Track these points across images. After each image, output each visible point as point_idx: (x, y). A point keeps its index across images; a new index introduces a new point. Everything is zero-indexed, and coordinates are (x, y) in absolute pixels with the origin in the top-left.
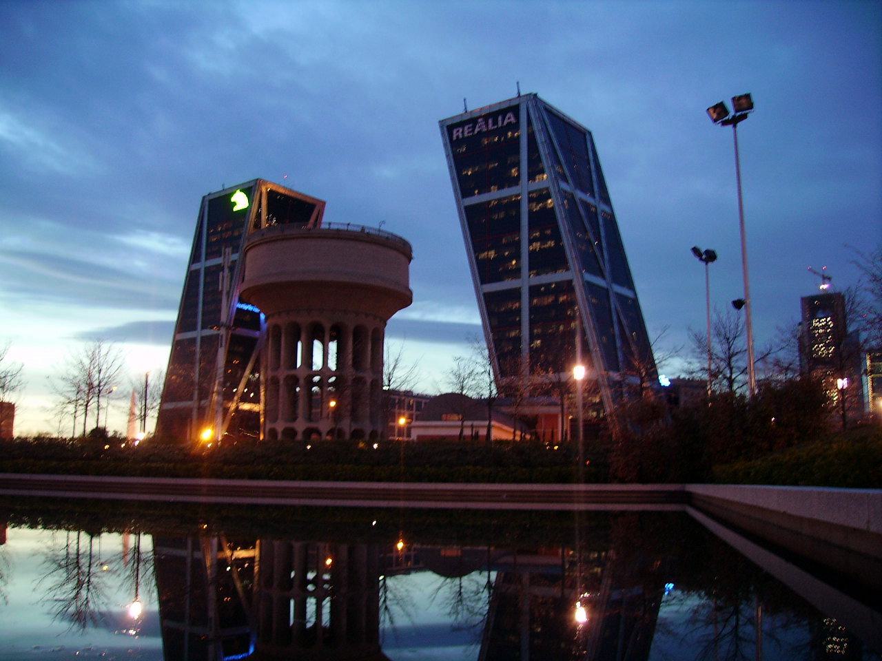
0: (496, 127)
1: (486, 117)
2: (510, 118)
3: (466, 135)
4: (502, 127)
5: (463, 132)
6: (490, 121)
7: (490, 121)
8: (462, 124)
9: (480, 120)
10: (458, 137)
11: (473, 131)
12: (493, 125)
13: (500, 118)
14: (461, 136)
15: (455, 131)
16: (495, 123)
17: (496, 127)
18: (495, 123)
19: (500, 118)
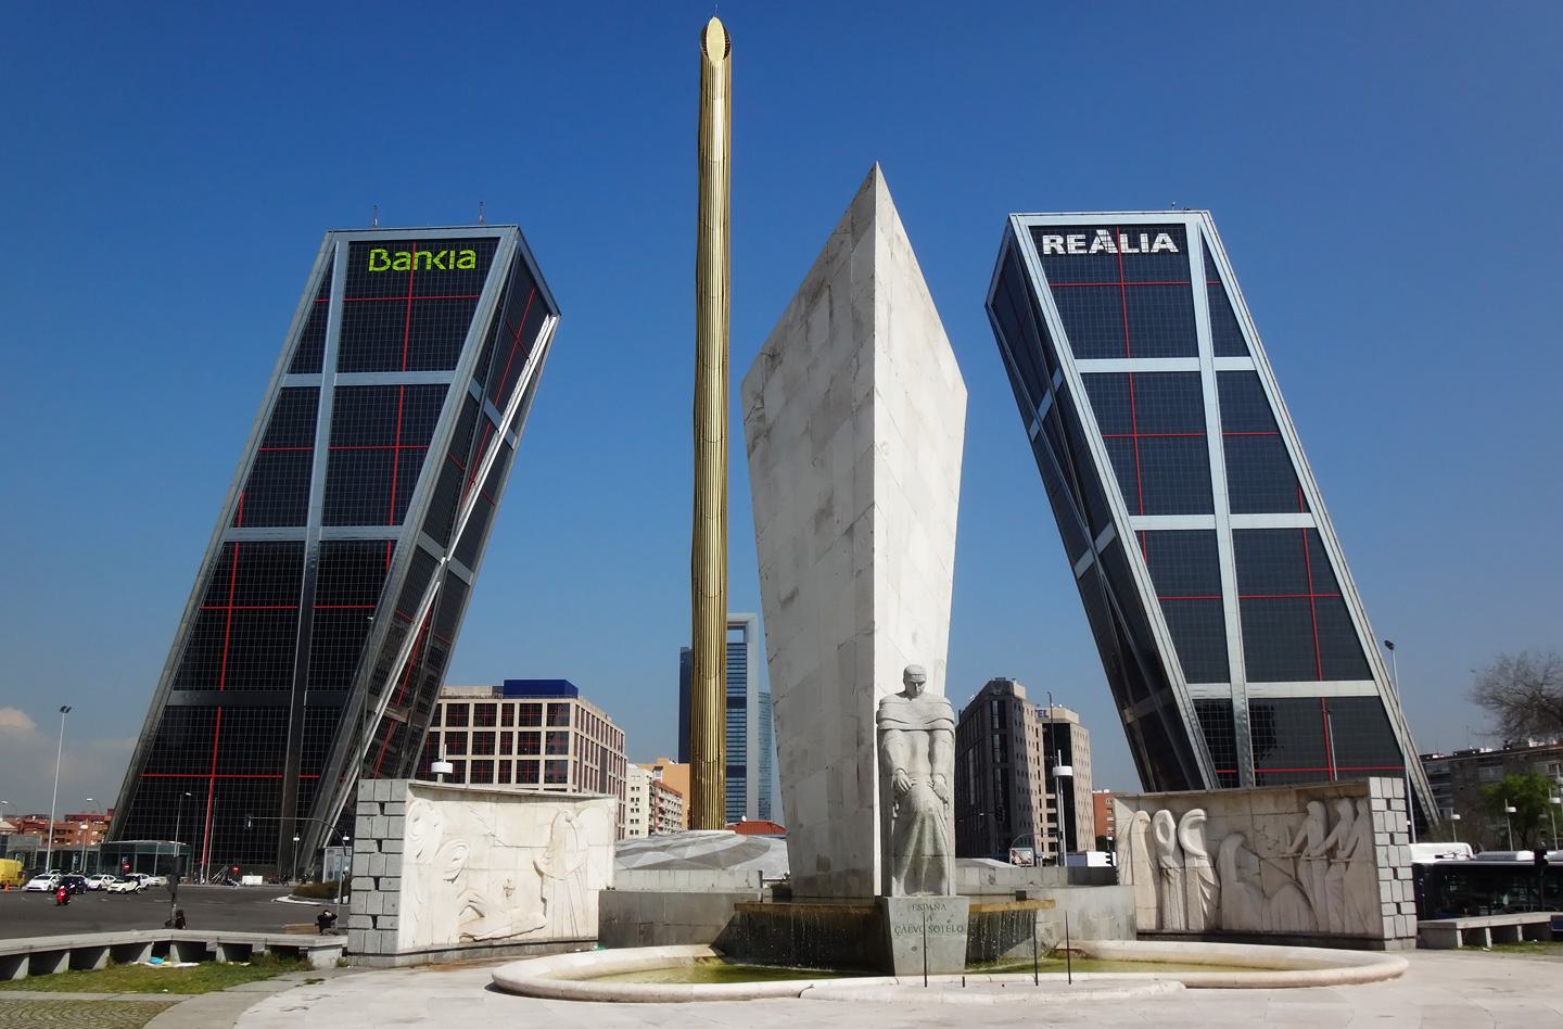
0: (1137, 251)
1: (1115, 230)
2: (1164, 242)
3: (1072, 250)
4: (1150, 253)
5: (1065, 246)
6: (1123, 239)
7: (1123, 239)
8: (1064, 230)
9: (1099, 232)
10: (1053, 248)
11: (1088, 247)
12: (1130, 247)
13: (1144, 238)
14: (1060, 250)
15: (1046, 239)
16: (1134, 242)
17: (1137, 251)
18: (1134, 242)
19: (1144, 238)
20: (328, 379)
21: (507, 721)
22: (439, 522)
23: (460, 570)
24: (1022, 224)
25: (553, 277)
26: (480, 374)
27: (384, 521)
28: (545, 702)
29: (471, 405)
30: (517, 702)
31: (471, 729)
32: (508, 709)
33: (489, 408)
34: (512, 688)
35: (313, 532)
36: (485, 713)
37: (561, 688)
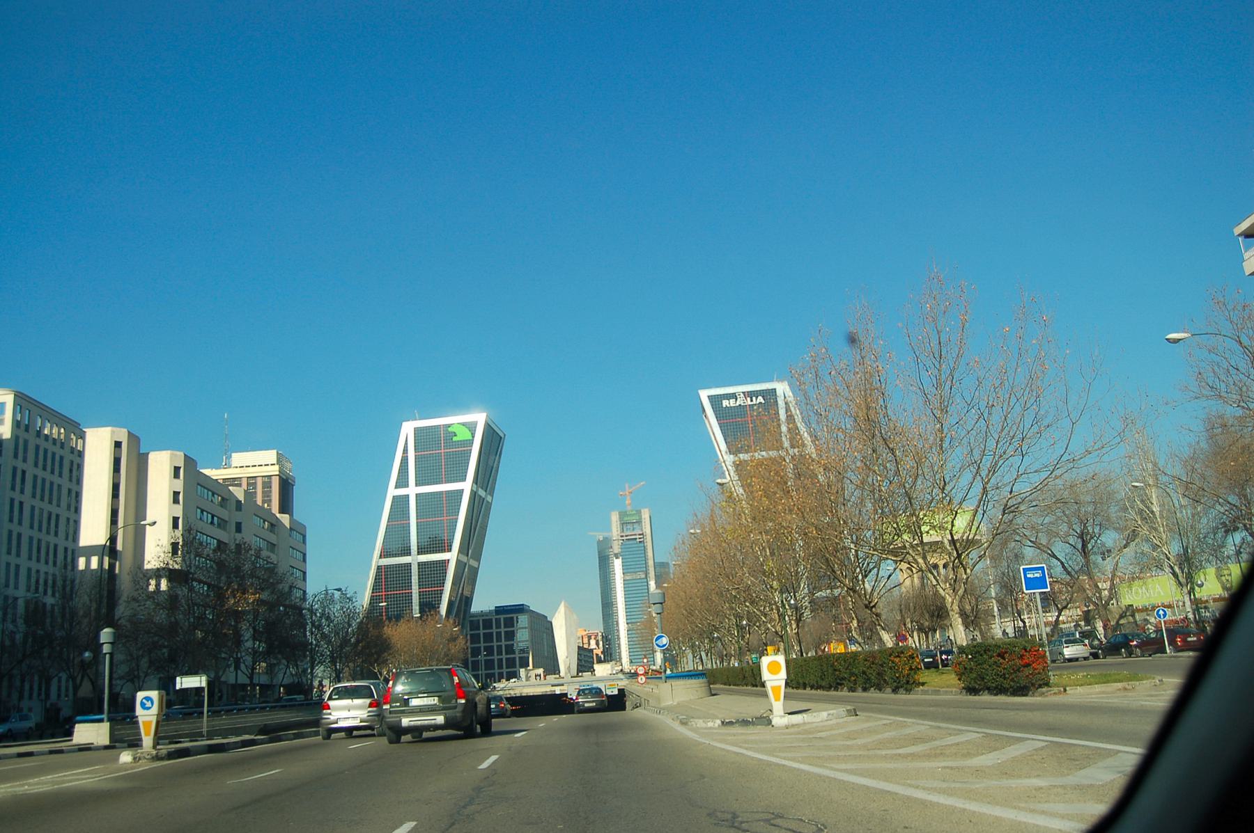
20: (412, 491)
21: (498, 626)
22: (464, 549)
23: (473, 563)
24: (704, 395)
25: (502, 428)
26: (476, 481)
27: (443, 551)
28: (514, 616)
29: (474, 495)
30: (502, 617)
31: (482, 632)
32: (498, 621)
33: (482, 493)
34: (500, 610)
35: (414, 559)
36: (487, 624)
37: (520, 609)
